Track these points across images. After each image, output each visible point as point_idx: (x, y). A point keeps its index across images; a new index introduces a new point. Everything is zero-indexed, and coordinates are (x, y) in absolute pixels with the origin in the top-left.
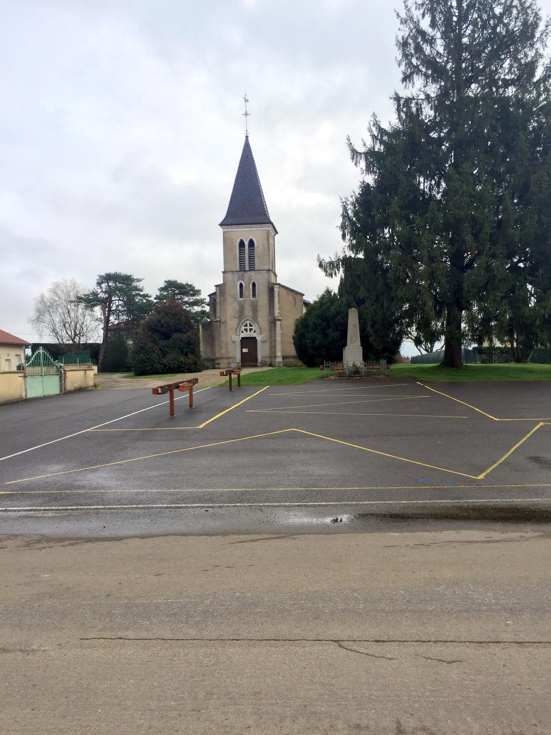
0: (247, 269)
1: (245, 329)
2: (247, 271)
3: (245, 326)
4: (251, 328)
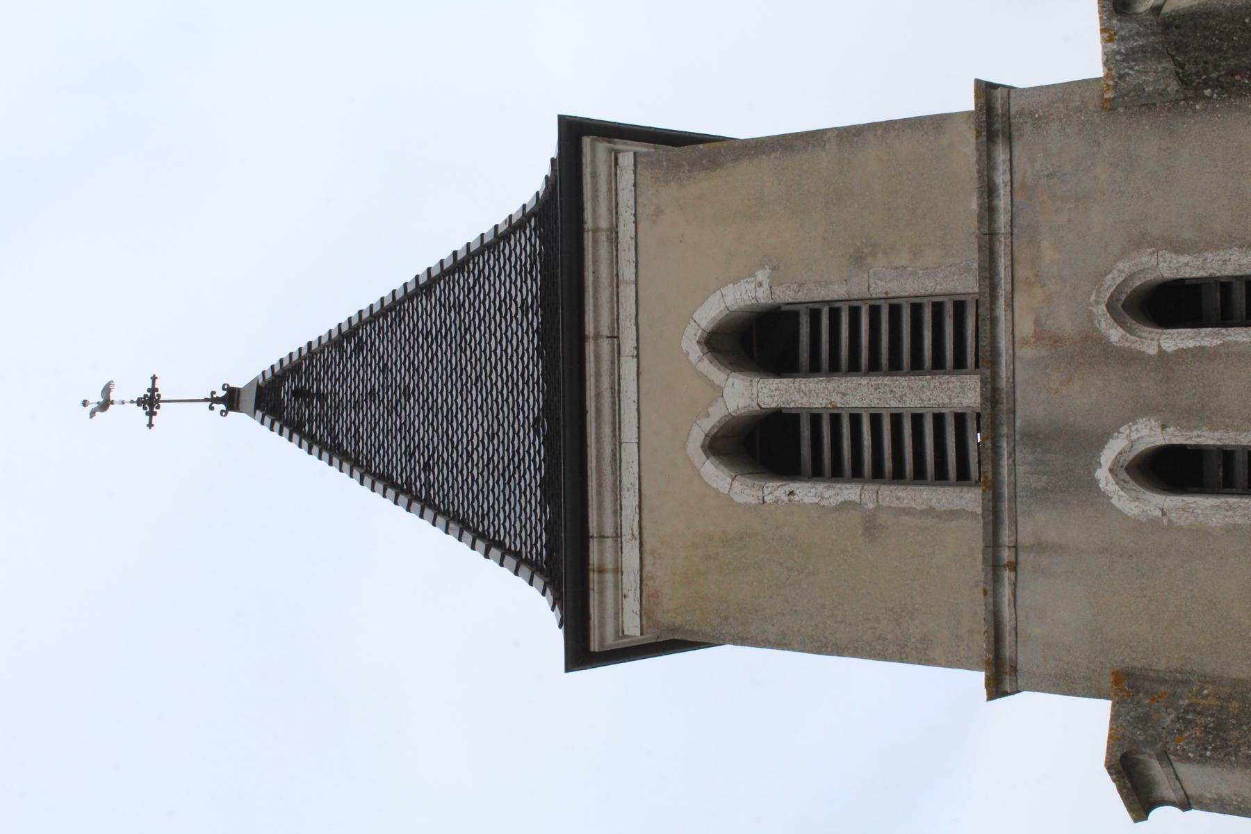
0: (957, 393)
2: (992, 395)
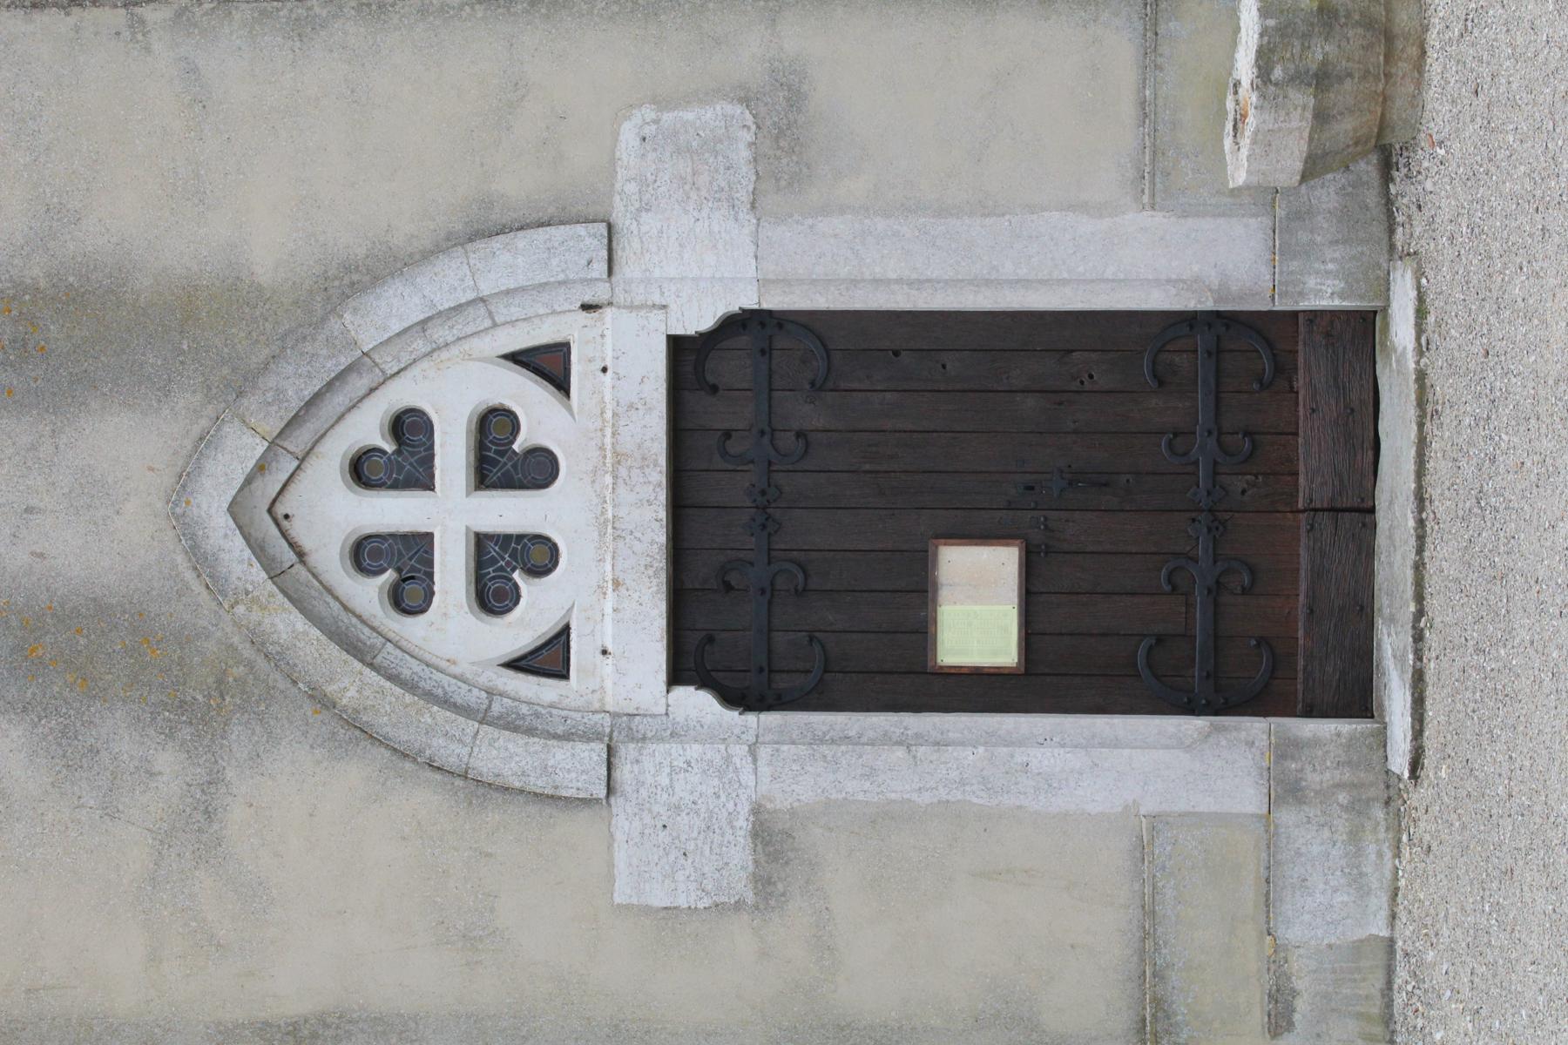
1: (493, 597)
3: (411, 595)
4: (452, 452)
